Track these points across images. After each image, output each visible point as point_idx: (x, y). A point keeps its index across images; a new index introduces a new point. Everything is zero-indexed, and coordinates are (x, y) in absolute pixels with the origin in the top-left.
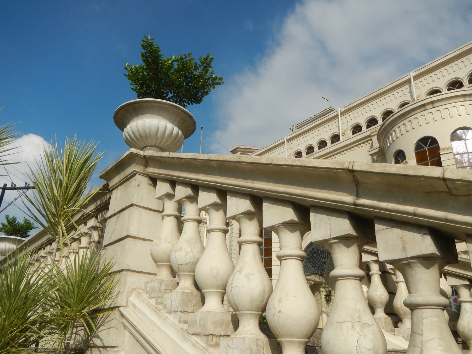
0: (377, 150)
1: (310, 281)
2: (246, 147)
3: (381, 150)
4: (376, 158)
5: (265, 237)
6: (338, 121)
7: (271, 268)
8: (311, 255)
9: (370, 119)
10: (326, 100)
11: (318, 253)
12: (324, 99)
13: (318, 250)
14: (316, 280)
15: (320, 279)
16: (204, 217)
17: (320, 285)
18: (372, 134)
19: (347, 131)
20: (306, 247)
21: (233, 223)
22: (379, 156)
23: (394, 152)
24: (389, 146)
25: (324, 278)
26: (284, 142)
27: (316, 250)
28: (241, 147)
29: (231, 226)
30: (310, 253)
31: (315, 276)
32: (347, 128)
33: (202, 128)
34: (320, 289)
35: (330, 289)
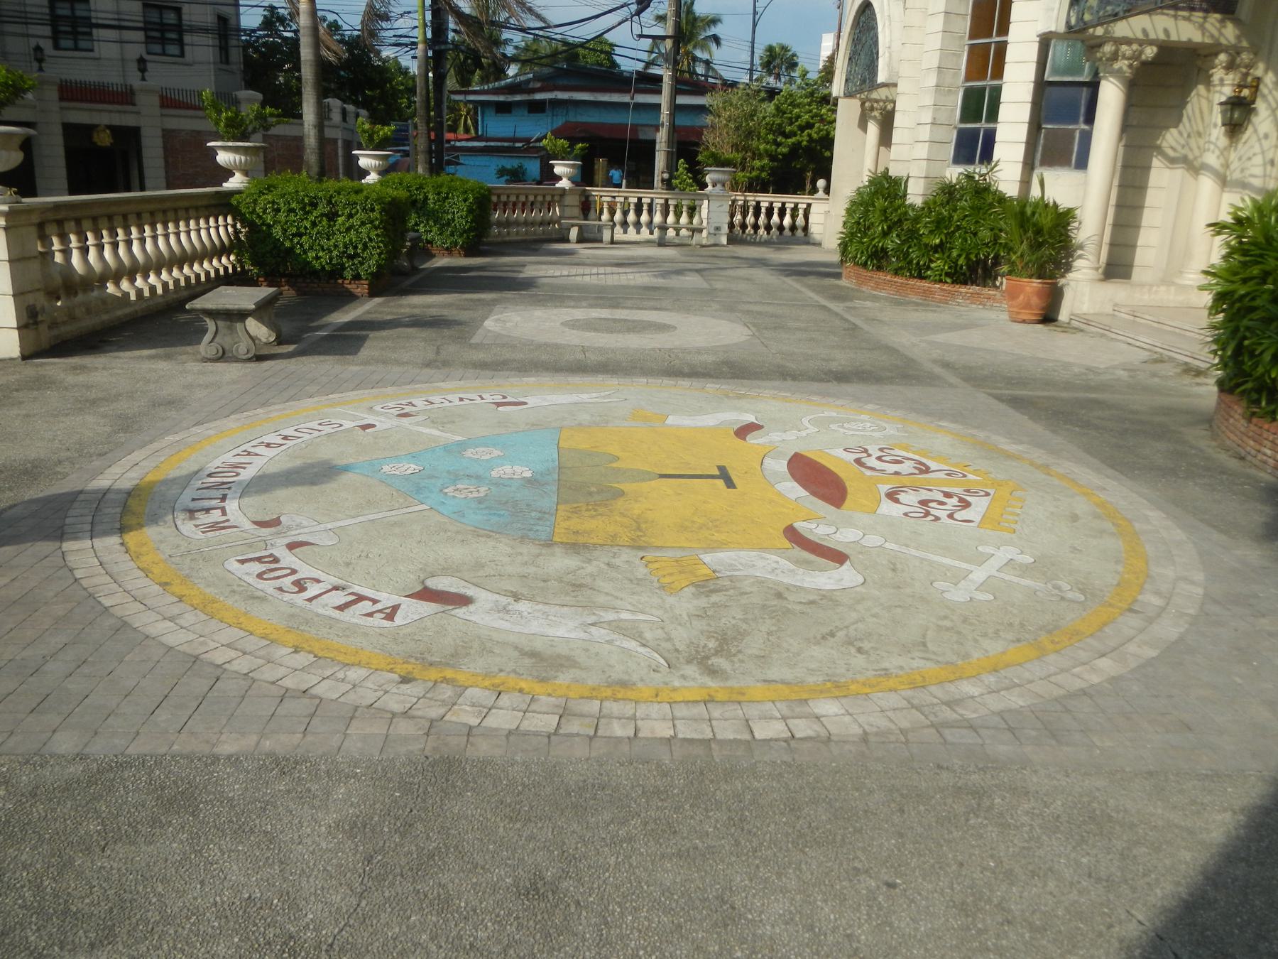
1: (1135, 47)
14: (1174, 37)
15: (1202, 27)
25: (1237, 22)
31: (1175, 17)
34: (1212, 75)
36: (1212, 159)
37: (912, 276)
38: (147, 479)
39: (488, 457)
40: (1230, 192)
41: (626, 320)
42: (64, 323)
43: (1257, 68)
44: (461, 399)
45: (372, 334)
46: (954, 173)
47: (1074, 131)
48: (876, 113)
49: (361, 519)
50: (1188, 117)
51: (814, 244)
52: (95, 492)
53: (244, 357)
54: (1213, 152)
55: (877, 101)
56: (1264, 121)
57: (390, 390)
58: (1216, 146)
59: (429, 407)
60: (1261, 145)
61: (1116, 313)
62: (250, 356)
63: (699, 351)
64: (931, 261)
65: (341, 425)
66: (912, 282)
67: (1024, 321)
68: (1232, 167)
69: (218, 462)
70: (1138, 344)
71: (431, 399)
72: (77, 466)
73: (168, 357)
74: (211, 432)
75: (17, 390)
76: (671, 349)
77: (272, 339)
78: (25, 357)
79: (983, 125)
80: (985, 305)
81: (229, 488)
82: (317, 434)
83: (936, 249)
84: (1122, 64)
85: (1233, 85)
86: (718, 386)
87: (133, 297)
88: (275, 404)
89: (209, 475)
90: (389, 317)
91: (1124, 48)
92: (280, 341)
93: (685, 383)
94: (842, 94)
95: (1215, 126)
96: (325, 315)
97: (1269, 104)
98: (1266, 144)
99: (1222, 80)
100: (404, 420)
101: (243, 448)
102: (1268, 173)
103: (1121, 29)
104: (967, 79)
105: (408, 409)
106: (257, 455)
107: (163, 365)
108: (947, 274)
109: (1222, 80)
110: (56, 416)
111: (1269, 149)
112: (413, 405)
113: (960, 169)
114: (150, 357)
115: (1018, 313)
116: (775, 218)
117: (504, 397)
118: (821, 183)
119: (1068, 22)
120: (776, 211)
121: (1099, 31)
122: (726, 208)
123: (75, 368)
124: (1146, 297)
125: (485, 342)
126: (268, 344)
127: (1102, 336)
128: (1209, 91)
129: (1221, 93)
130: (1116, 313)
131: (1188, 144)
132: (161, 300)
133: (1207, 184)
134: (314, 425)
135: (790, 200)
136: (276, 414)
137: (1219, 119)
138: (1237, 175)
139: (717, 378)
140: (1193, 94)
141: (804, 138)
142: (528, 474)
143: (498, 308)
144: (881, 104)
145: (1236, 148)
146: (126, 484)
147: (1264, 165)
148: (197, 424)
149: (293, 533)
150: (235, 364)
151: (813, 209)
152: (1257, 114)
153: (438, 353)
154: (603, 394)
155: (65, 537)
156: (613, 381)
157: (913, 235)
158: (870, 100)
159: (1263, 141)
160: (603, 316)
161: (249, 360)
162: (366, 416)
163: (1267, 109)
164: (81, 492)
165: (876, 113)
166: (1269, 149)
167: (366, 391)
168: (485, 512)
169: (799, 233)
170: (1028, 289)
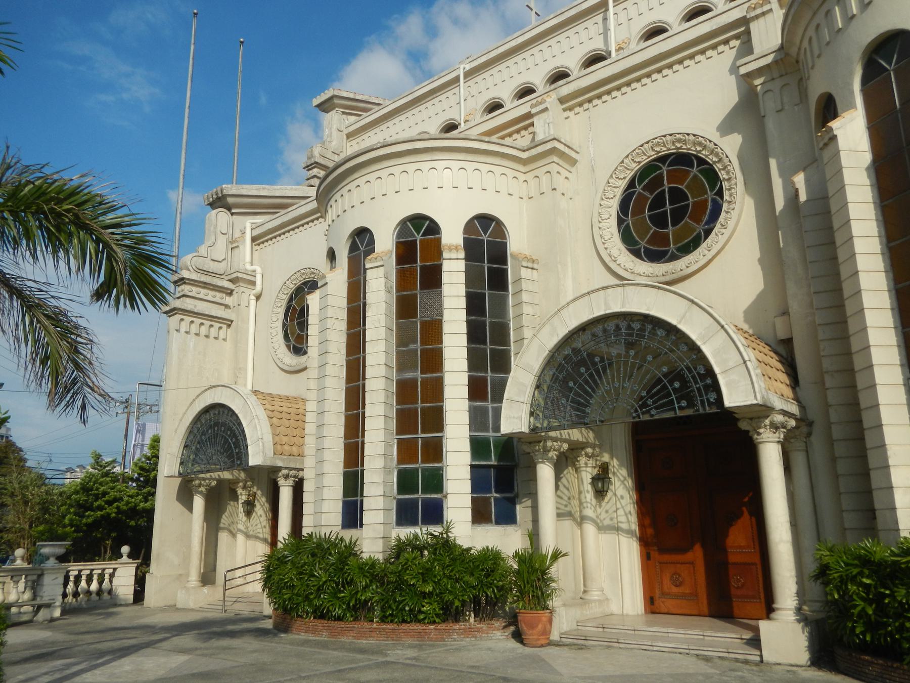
0: (769, 59)
2: (357, 97)
3: (781, 59)
4: (761, 84)
5: (423, 319)
6: (605, 19)
7: (441, 404)
8: (570, 369)
9: (695, 11)
10: (536, 13)
11: (594, 364)
12: (532, 10)
13: (591, 356)
14: (572, 439)
15: (581, 432)
16: (249, 267)
17: (577, 449)
18: (753, 14)
19: (629, 43)
20: (556, 345)
21: (328, 280)
22: (773, 79)
23: (870, 39)
24: (840, 26)
25: (591, 429)
26: (456, 80)
27: (585, 354)
28: (345, 94)
29: (322, 286)
30: (566, 365)
32: (629, 37)
33: (242, 42)
35: (606, 458)
36: (589, 512)
37: (404, 621)
40: (605, 533)
43: (603, 457)
46: (405, 532)
47: (489, 498)
48: (202, 489)
50: (565, 486)
51: (121, 605)
54: (591, 508)
55: (204, 479)
56: (619, 487)
58: (591, 504)
60: (620, 502)
61: (580, 628)
64: (423, 606)
66: (405, 626)
67: (542, 646)
68: (602, 517)
70: (655, 649)
79: (420, 496)
80: (476, 637)
83: (424, 595)
84: (553, 454)
85: (593, 467)
91: (555, 444)
94: (177, 474)
95: (588, 492)
97: (619, 478)
98: (623, 502)
99: (586, 464)
102: (630, 519)
103: (552, 434)
104: (400, 461)
108: (438, 615)
109: (586, 464)
111: (627, 505)
113: (417, 530)
115: (538, 639)
116: (83, 584)
118: (125, 549)
119: (530, 426)
120: (84, 578)
121: (543, 434)
122: (61, 580)
124: (588, 613)
127: (609, 647)
128: (573, 470)
129: (586, 471)
130: (580, 628)
131: (570, 504)
133: (590, 528)
135: (97, 567)
137: (589, 487)
138: (607, 522)
140: (565, 472)
141: (111, 511)
144: (207, 481)
145: (600, 506)
147: (626, 515)
151: (117, 573)
152: (612, 484)
157: (400, 585)
158: (199, 479)
159: (621, 501)
163: (618, 481)
165: (202, 489)
166: (627, 505)
169: (106, 596)
170: (544, 619)
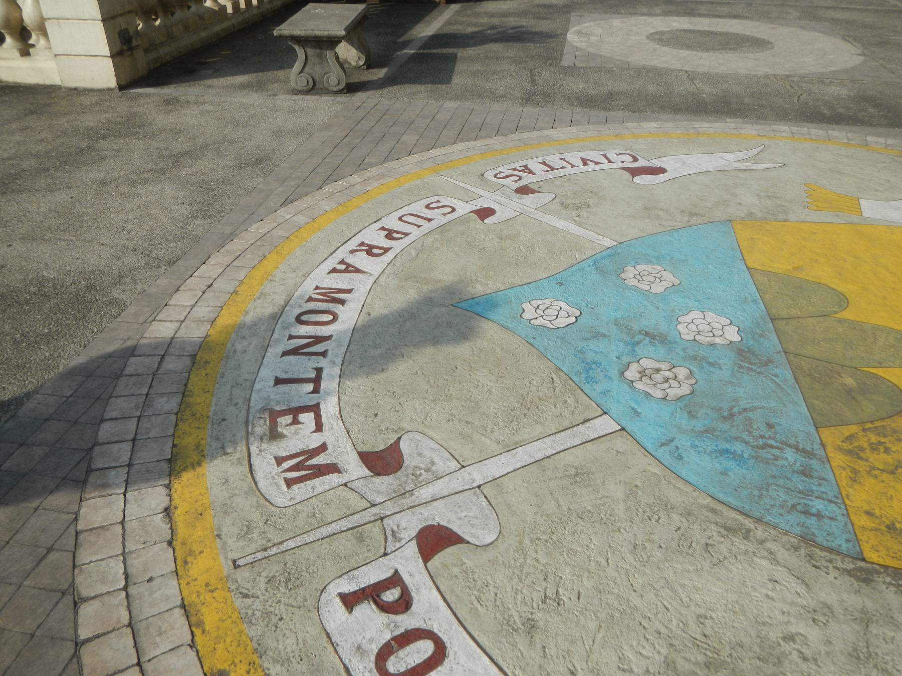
38: (221, 322)
39: (658, 288)
41: (712, 33)
42: (162, 44)
44: (585, 162)
45: (461, 53)
49: (522, 456)
52: (156, 346)
53: (335, 89)
57: (496, 142)
59: (550, 175)
62: (341, 87)
63: (822, 79)
65: (454, 210)
69: (308, 288)
71: (550, 159)
72: (139, 287)
73: (259, 86)
74: (301, 219)
75: (104, 137)
76: (787, 77)
77: (361, 63)
78: (123, 87)
81: (324, 354)
82: (426, 226)
86: (882, 140)
87: (230, 10)
88: (372, 165)
89: (299, 320)
90: (470, 30)
92: (370, 64)
93: (838, 133)
96: (410, 28)
100: (528, 199)
101: (340, 254)
105: (527, 179)
106: (357, 271)
107: (254, 99)
110: (133, 184)
112: (531, 172)
114: (244, 87)
117: (635, 160)
123: (167, 102)
125: (580, 64)
126: (358, 68)
132: (256, 11)
134: (418, 208)
136: (375, 184)
139: (871, 125)
142: (732, 335)
143: (574, 16)
146: (195, 333)
148: (287, 202)
149: (425, 493)
150: (325, 98)
153: (533, 81)
154: (751, 153)
155: (91, 479)
156: (750, 130)
160: (686, 27)
161: (340, 92)
162: (480, 192)
164: (132, 352)
167: (472, 144)
168: (709, 445)
